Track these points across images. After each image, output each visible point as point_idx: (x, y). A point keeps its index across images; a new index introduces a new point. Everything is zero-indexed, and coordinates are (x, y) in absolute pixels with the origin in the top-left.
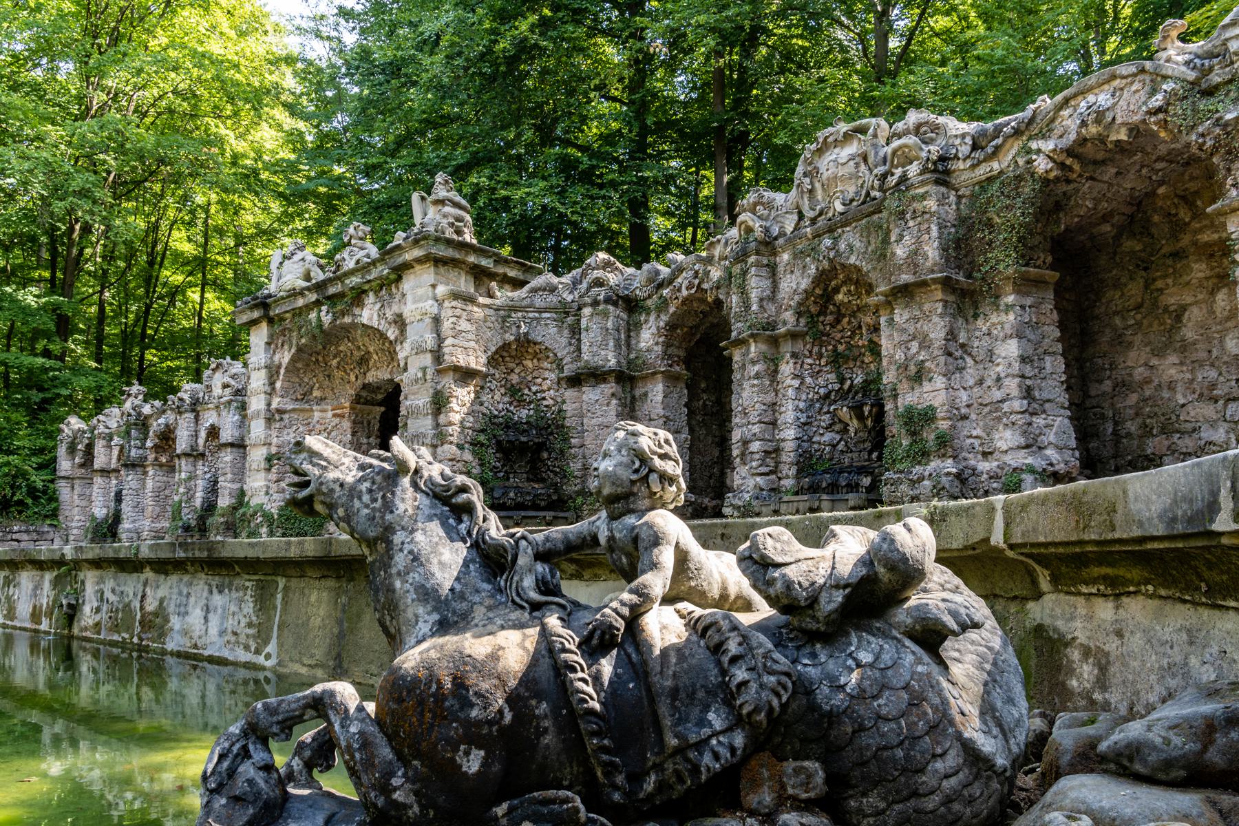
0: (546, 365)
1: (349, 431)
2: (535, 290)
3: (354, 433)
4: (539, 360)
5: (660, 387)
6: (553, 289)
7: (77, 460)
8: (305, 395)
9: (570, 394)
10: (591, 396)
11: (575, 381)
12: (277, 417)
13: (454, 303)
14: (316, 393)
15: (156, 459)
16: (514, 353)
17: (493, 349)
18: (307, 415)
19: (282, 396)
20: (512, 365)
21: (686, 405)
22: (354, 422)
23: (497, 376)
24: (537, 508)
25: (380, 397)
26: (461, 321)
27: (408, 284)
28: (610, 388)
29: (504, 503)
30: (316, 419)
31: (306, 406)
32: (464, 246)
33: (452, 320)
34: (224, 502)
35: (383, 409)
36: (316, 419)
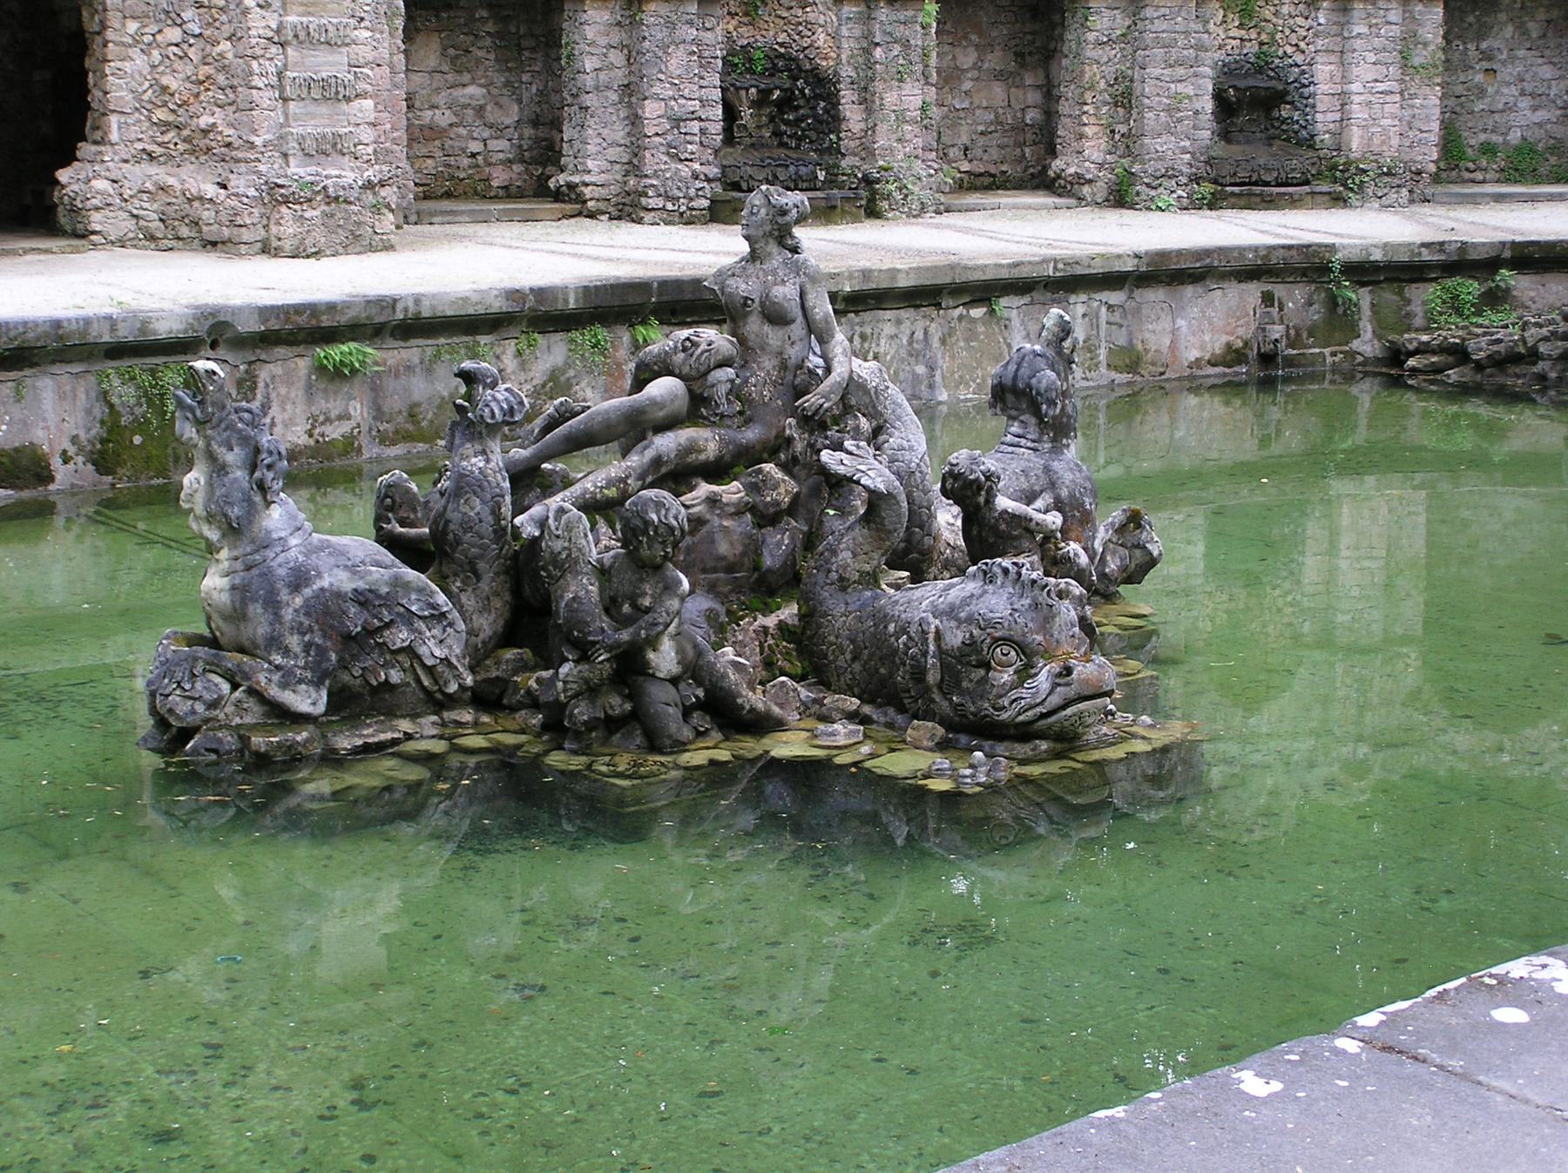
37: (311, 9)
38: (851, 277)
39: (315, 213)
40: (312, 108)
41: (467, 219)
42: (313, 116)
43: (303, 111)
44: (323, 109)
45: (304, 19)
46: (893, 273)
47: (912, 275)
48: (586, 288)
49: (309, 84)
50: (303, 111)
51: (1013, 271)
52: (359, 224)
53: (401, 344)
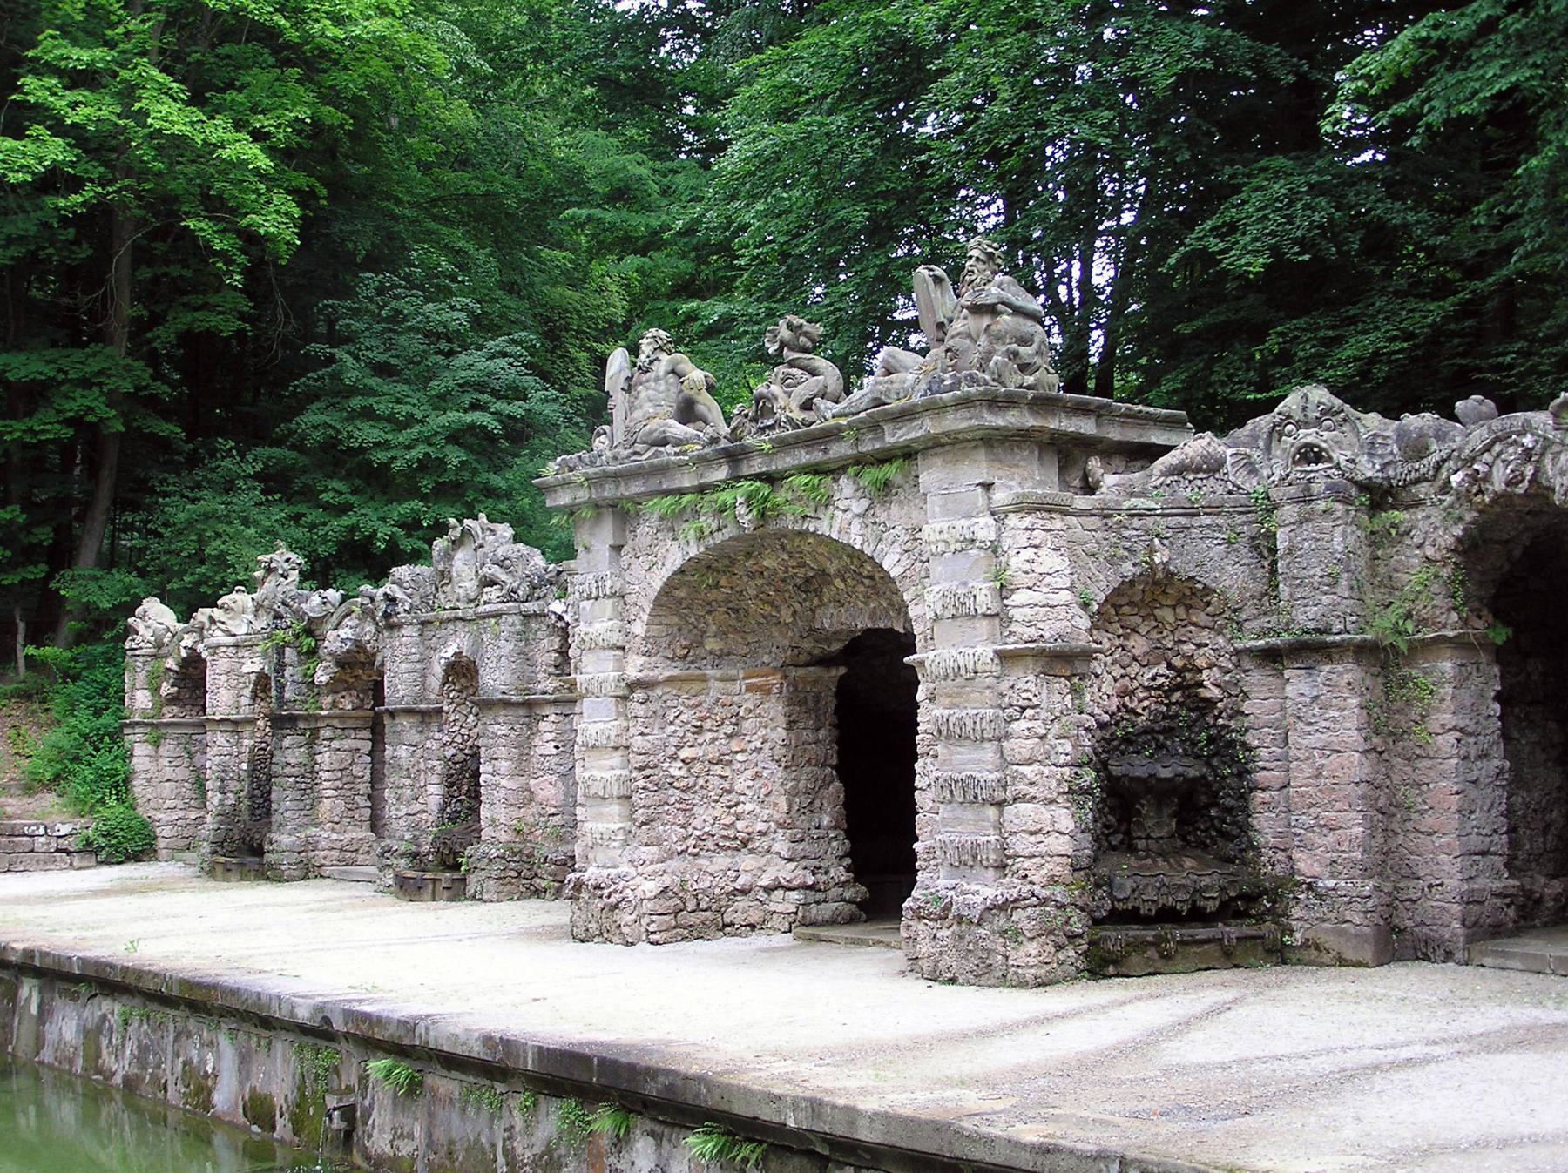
0: (1201, 618)
1: (782, 721)
2: (1179, 471)
3: (790, 726)
4: (1188, 608)
5: (1447, 666)
6: (1213, 467)
7: (166, 689)
8: (688, 647)
9: (1256, 678)
10: (1304, 687)
11: (1271, 657)
13: (1028, 521)
14: (712, 644)
15: (334, 705)
16: (1137, 599)
17: (1101, 597)
18: (696, 687)
19: (647, 654)
21: (1498, 697)
22: (791, 702)
24: (1197, 916)
25: (836, 646)
26: (1043, 552)
28: (1345, 673)
29: (1136, 909)
32: (1043, 404)
34: (496, 813)
35: (843, 671)
37: (956, 700)
38: (795, 1108)
39: (948, 933)
40: (959, 812)
41: (1519, 965)
42: (960, 821)
43: (951, 815)
44: (969, 814)
45: (946, 712)
46: (851, 1113)
47: (877, 1125)
48: (540, 1048)
49: (950, 784)
50: (951, 815)
51: (1040, 1160)
52: (989, 951)
53: (445, 1073)
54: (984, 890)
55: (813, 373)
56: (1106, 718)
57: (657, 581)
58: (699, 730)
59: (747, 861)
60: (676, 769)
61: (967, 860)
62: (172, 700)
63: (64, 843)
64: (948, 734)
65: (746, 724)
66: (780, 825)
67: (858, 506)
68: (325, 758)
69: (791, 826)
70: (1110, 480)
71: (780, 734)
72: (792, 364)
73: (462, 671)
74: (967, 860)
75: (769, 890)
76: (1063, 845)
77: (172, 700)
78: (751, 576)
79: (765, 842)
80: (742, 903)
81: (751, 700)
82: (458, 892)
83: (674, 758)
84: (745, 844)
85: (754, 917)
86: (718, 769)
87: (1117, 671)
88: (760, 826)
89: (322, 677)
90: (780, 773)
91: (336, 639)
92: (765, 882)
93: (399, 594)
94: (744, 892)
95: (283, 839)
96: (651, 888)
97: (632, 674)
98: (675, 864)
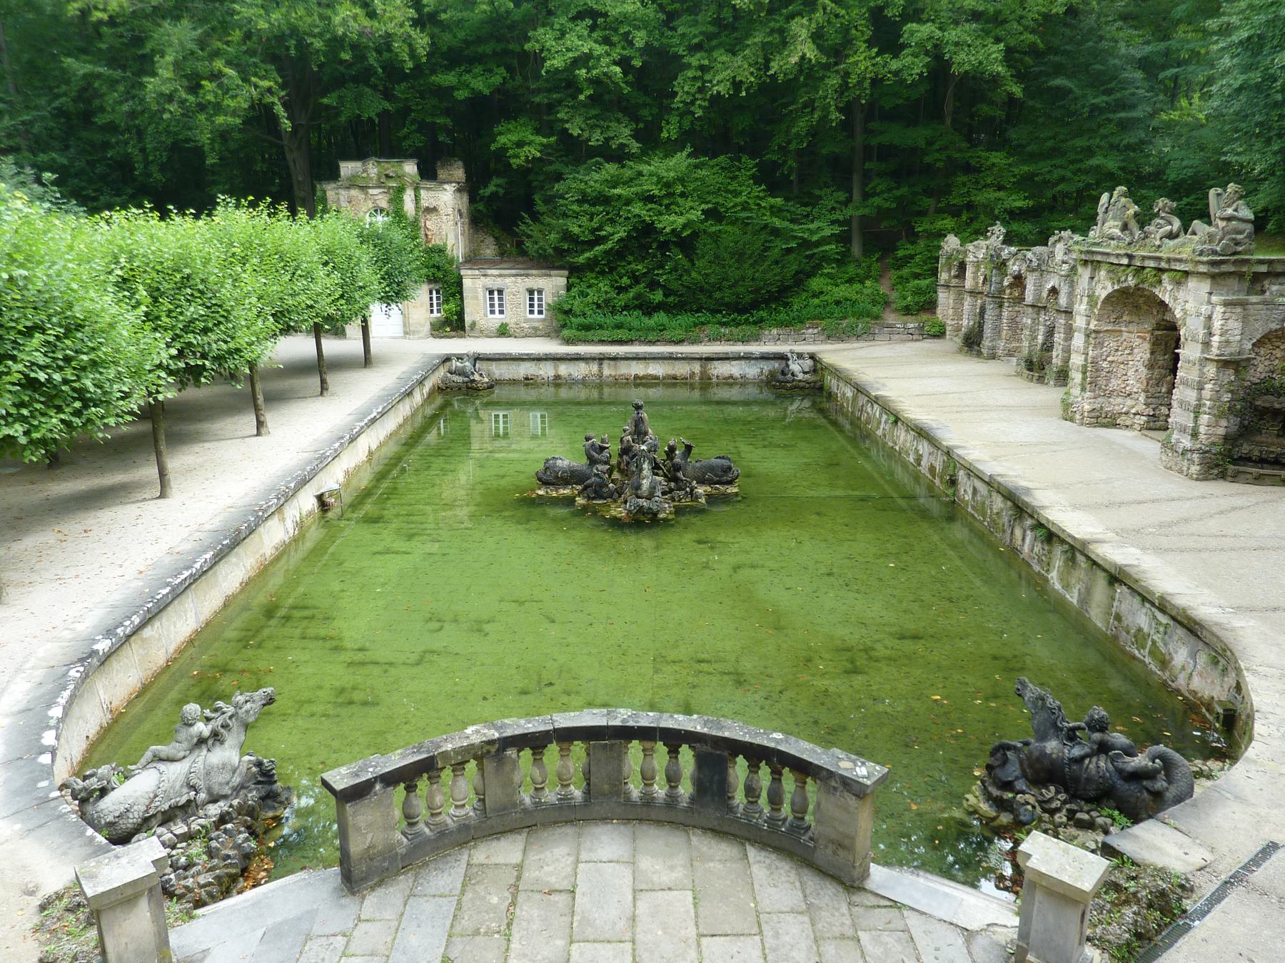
1: (1148, 351)
3: (1152, 353)
12: (1093, 335)
14: (1125, 318)
17: (1259, 336)
18: (1117, 334)
19: (1098, 320)
20: (1277, 344)
22: (1154, 344)
23: (1262, 353)
27: (1192, 283)
30: (1124, 337)
31: (1117, 328)
33: (1220, 322)
36: (1124, 337)
54: (1186, 442)
55: (1170, 223)
56: (1258, 381)
57: (1104, 294)
58: (1117, 350)
59: (1129, 402)
60: (1105, 365)
61: (1183, 430)
62: (956, 277)
63: (910, 331)
64: (1185, 383)
65: (1135, 351)
66: (1144, 391)
67: (1169, 287)
68: (1005, 314)
69: (1148, 391)
70: (1274, 288)
71: (1148, 355)
72: (1162, 218)
73: (1054, 291)
74: (1183, 430)
75: (1135, 414)
76: (1221, 431)
77: (956, 277)
78: (1141, 297)
79: (1137, 396)
80: (1124, 417)
81: (1138, 341)
82: (1041, 380)
83: (1105, 360)
84: (1129, 395)
85: (1128, 423)
86: (1122, 366)
87: (1267, 363)
88: (1135, 390)
89: (1006, 283)
90: (1145, 371)
91: (1014, 267)
92: (1133, 411)
93: (1034, 260)
94: (1126, 413)
95: (986, 343)
96: (1087, 407)
97: (1092, 327)
98: (1100, 399)
